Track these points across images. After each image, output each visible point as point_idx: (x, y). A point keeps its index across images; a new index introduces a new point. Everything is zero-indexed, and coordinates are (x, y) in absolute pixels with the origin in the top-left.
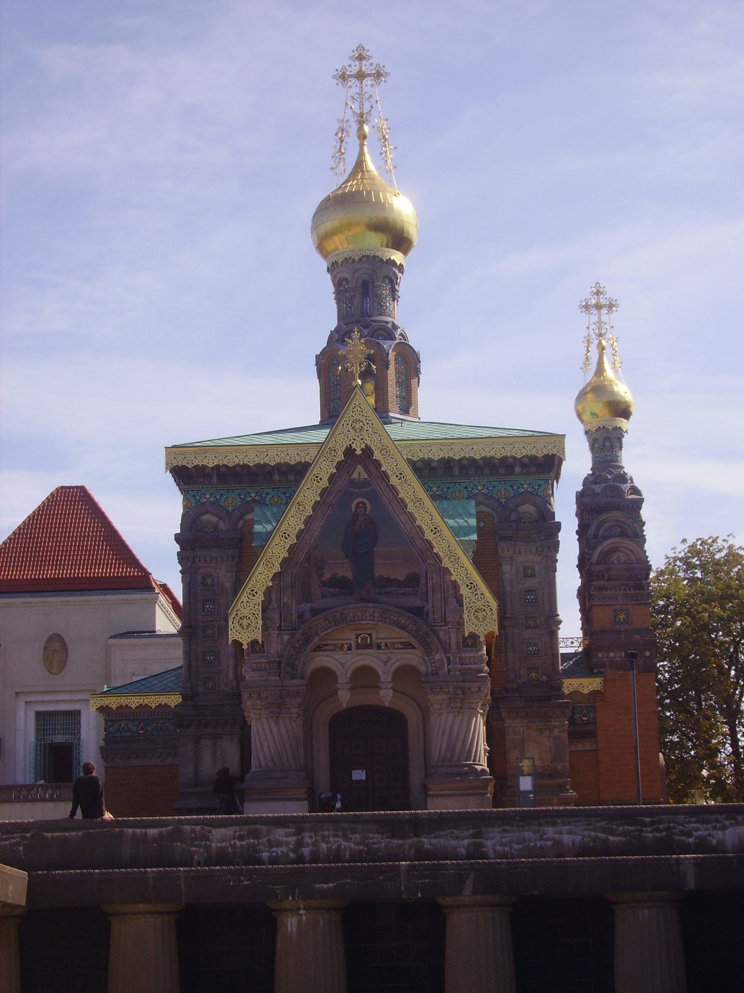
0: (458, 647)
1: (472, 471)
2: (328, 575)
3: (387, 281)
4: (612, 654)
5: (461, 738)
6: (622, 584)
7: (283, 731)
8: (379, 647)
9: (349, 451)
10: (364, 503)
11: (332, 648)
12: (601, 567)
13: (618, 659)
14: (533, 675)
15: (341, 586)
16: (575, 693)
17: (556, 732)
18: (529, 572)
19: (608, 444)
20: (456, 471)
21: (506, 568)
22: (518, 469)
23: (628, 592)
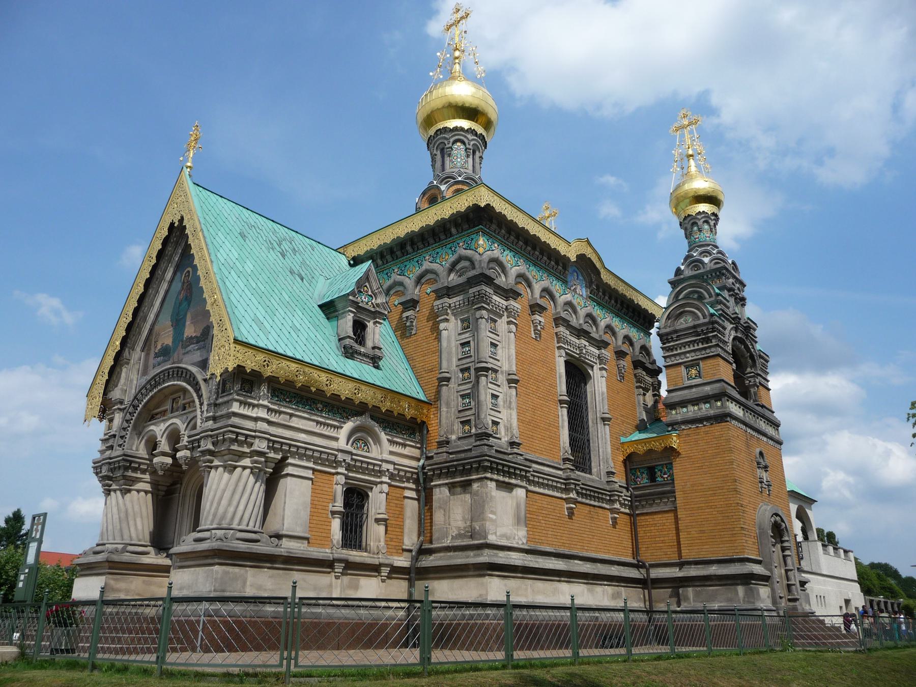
0: (217, 393)
1: (420, 245)
2: (159, 347)
3: (459, 144)
4: (685, 410)
5: (210, 497)
6: (690, 342)
7: (114, 502)
8: (184, 409)
9: (172, 226)
10: (188, 272)
11: (158, 416)
12: (668, 330)
13: (690, 413)
14: (467, 427)
15: (165, 352)
16: (650, 451)
17: (475, 486)
18: (465, 324)
19: (695, 228)
20: (409, 248)
21: (442, 326)
22: (453, 230)
23: (696, 347)
